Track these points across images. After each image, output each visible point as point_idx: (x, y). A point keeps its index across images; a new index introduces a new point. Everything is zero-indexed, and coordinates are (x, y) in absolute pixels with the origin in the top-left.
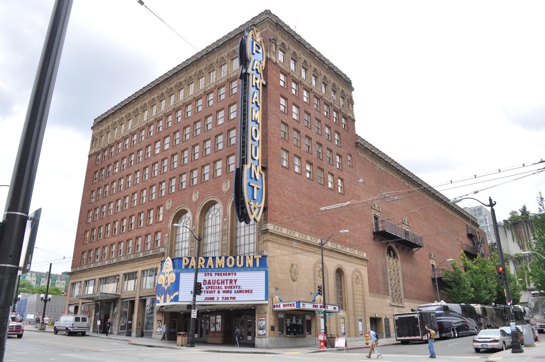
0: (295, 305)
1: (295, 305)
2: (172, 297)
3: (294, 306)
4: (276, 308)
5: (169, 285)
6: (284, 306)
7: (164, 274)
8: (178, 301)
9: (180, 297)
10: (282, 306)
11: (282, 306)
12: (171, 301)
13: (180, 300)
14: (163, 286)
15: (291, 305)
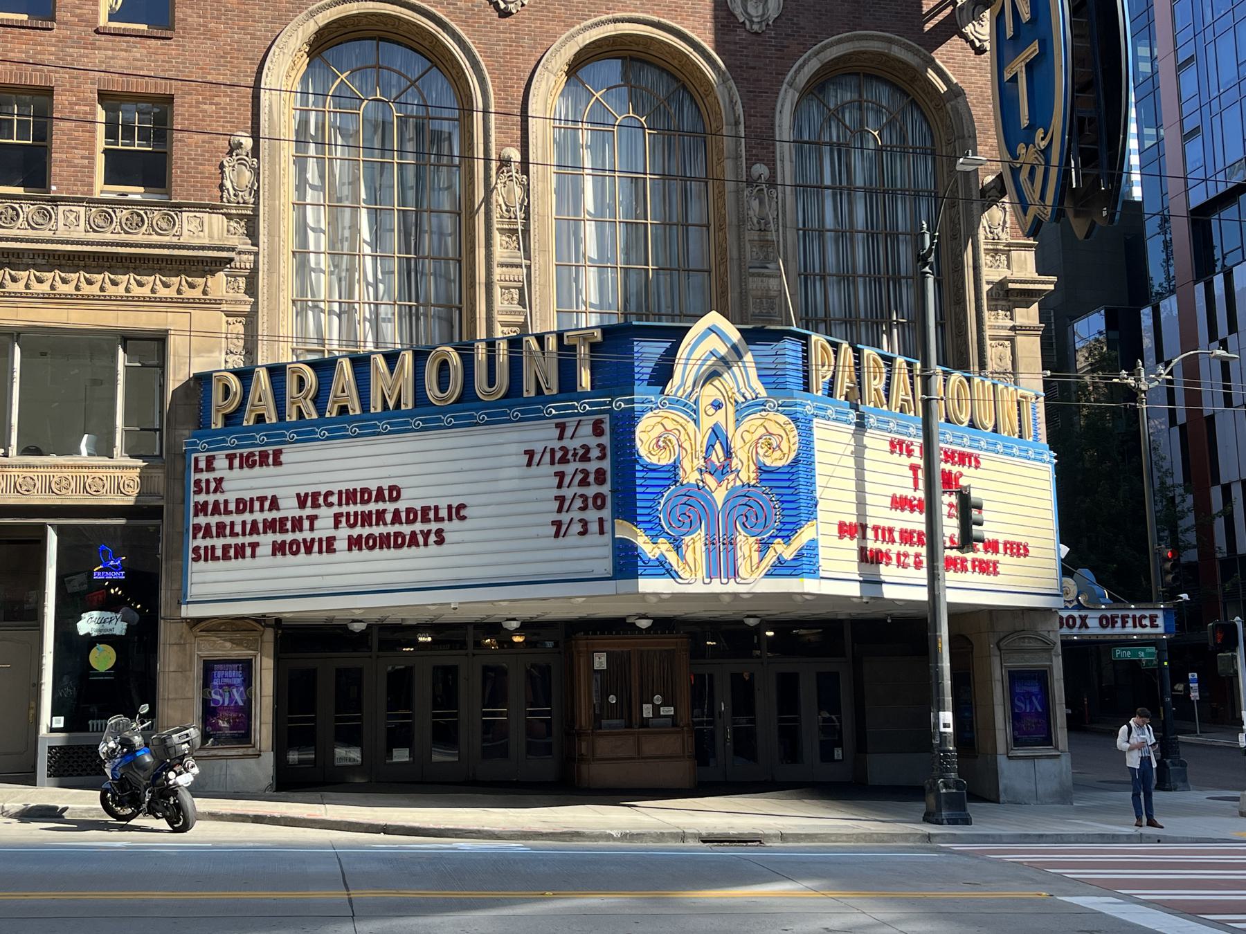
0: (1160, 621)
1: (1160, 621)
2: (788, 553)
3: (1153, 626)
4: (1065, 631)
5: (748, 474)
6: (1106, 622)
7: (693, 412)
8: (814, 573)
9: (822, 552)
10: (1093, 623)
11: (1093, 623)
12: (781, 569)
13: (825, 566)
14: (690, 476)
15: (1138, 622)
